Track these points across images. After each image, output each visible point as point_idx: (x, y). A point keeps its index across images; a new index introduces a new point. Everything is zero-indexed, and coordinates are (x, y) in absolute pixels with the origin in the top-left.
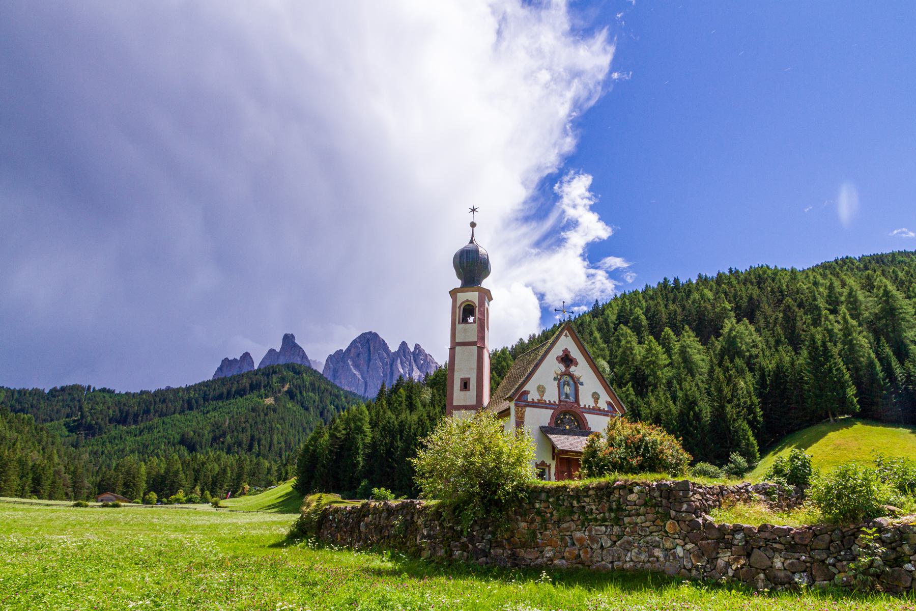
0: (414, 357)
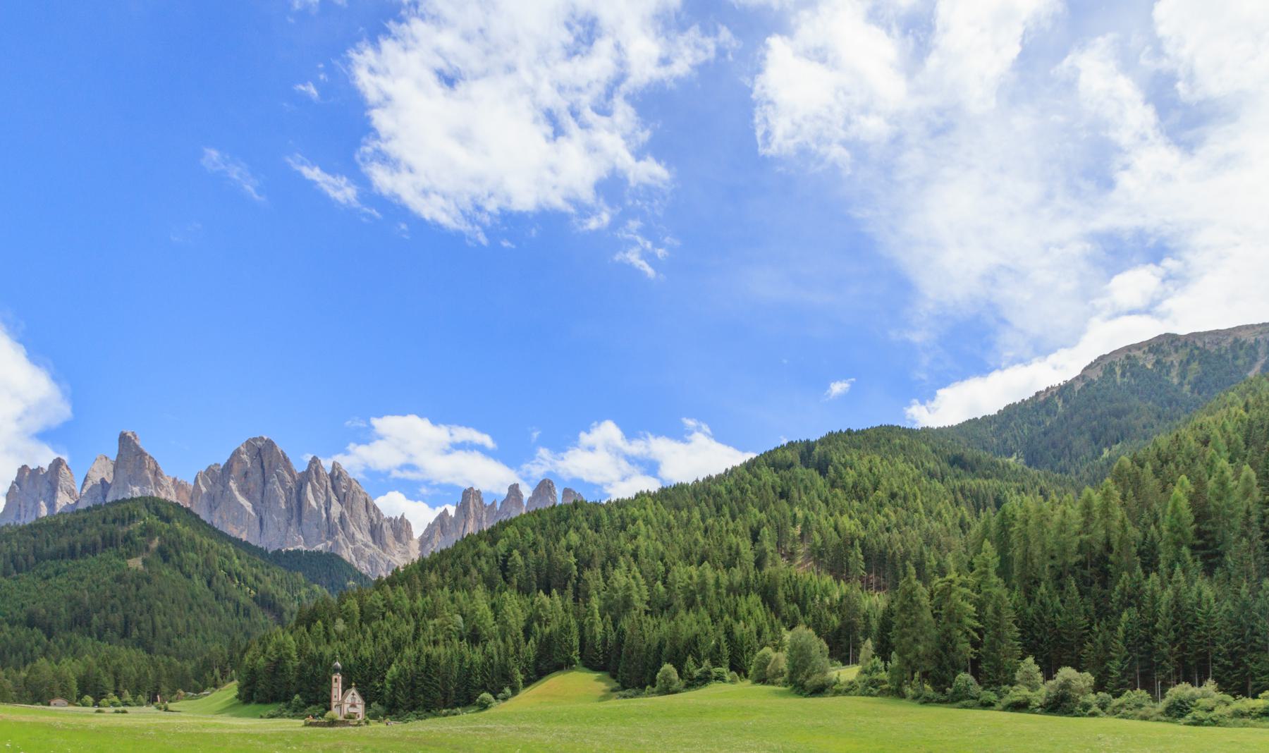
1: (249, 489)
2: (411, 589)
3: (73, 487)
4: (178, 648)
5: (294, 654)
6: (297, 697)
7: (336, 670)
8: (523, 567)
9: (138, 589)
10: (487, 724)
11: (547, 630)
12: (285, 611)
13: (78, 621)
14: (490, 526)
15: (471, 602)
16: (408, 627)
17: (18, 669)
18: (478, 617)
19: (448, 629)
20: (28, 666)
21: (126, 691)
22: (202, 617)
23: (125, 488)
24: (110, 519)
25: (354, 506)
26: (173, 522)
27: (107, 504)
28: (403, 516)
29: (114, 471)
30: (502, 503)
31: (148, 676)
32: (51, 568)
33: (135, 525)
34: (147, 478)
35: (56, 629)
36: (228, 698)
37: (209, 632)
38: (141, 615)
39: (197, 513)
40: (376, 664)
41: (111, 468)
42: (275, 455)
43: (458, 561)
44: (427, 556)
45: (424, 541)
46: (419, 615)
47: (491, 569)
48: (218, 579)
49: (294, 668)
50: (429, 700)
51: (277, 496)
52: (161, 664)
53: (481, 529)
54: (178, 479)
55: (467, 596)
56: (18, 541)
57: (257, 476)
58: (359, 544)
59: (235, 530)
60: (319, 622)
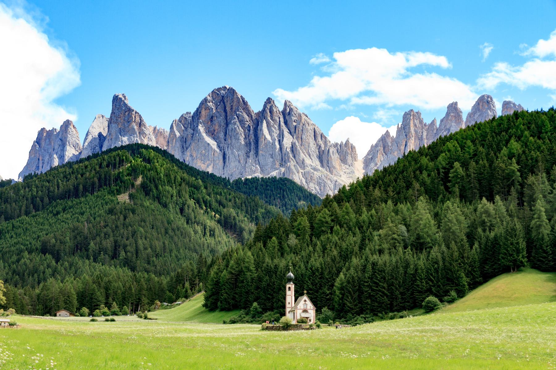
0: (284, 118)
1: (214, 130)
2: (356, 205)
3: (78, 142)
4: (156, 266)
5: (252, 267)
6: (255, 304)
7: (290, 280)
8: (465, 177)
9: (125, 219)
10: (433, 326)
11: (492, 234)
12: (244, 230)
13: (79, 247)
14: (430, 142)
15: (415, 213)
16: (355, 239)
17: (33, 287)
18: (421, 226)
19: (393, 239)
20: (41, 285)
21: (114, 303)
22: (176, 238)
23: (117, 138)
24: (105, 163)
25: (304, 137)
26: (154, 162)
27: (103, 152)
28: (347, 141)
29: (109, 126)
30: (442, 121)
31: (131, 290)
32: (60, 205)
33: (124, 167)
34: (134, 129)
35: (62, 254)
36: (195, 307)
37: (181, 251)
38: (127, 240)
39: (172, 154)
40: (326, 273)
41: (106, 124)
42: (235, 100)
43: (400, 176)
44: (371, 174)
45: (367, 161)
46: (365, 228)
47: (432, 182)
48: (188, 207)
49: (252, 279)
50: (376, 304)
51: (237, 134)
52: (142, 280)
53: (422, 146)
54: (158, 128)
55: (410, 208)
56: (37, 187)
57: (222, 119)
58: (308, 169)
59: (202, 165)
60: (274, 238)
